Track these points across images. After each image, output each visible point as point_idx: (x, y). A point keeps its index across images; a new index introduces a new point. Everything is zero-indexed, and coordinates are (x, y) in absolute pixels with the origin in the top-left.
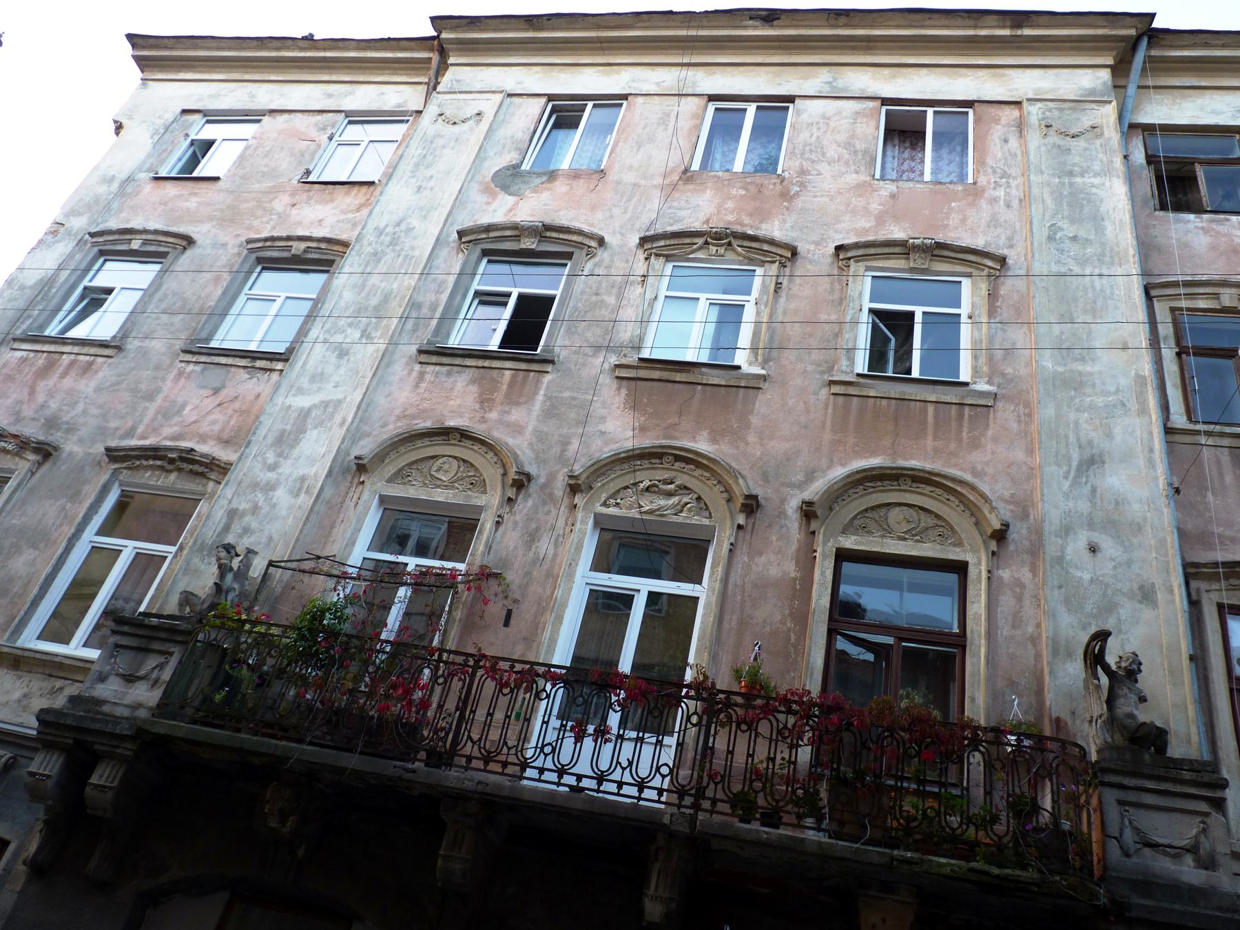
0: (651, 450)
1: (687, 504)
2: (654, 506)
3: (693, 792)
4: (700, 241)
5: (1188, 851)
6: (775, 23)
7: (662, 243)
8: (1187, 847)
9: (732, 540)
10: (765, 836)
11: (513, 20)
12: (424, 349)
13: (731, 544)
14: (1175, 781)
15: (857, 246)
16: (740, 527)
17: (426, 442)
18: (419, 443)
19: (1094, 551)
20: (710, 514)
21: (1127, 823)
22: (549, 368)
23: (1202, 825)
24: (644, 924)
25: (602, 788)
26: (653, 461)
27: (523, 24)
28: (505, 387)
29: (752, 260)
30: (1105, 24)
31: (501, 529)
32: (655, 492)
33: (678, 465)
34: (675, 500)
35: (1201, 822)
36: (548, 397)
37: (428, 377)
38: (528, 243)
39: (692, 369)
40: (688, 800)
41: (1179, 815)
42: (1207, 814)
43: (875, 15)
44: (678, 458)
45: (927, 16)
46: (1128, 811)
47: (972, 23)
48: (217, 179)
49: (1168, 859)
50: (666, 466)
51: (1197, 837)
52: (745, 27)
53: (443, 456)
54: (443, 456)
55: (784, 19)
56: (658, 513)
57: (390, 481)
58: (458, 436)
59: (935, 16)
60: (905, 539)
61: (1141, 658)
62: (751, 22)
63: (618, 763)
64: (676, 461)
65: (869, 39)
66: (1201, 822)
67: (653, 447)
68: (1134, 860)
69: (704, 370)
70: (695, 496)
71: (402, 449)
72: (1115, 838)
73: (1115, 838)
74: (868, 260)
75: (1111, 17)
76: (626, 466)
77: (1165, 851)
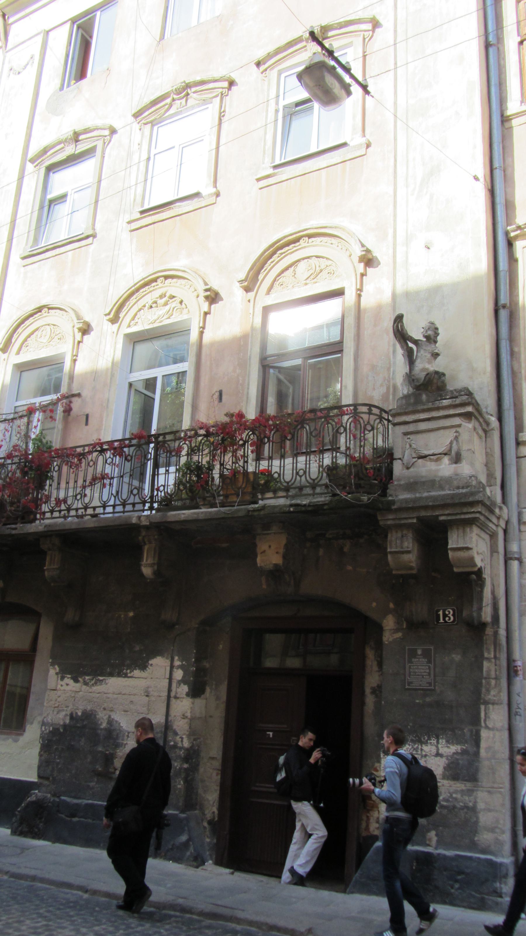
1: (174, 308)
2: (155, 317)
3: (149, 500)
4: (168, 101)
5: (445, 454)
8: (444, 452)
10: (183, 516)
12: (22, 256)
14: (438, 409)
15: (269, 56)
17: (31, 320)
19: (428, 248)
20: (189, 311)
21: (408, 446)
23: (455, 434)
24: (148, 581)
25: (106, 511)
29: (204, 100)
34: (167, 308)
35: (455, 432)
38: (70, 150)
39: (172, 206)
40: (147, 505)
41: (442, 431)
42: (459, 426)
44: (166, 277)
46: (409, 438)
49: (433, 463)
51: (451, 443)
53: (42, 326)
54: (42, 326)
56: (158, 321)
58: (46, 309)
60: (306, 284)
61: (438, 326)
63: (112, 494)
66: (455, 432)
68: (411, 470)
69: (178, 204)
70: (180, 300)
72: (400, 459)
73: (400, 459)
74: (277, 66)
77: (430, 459)
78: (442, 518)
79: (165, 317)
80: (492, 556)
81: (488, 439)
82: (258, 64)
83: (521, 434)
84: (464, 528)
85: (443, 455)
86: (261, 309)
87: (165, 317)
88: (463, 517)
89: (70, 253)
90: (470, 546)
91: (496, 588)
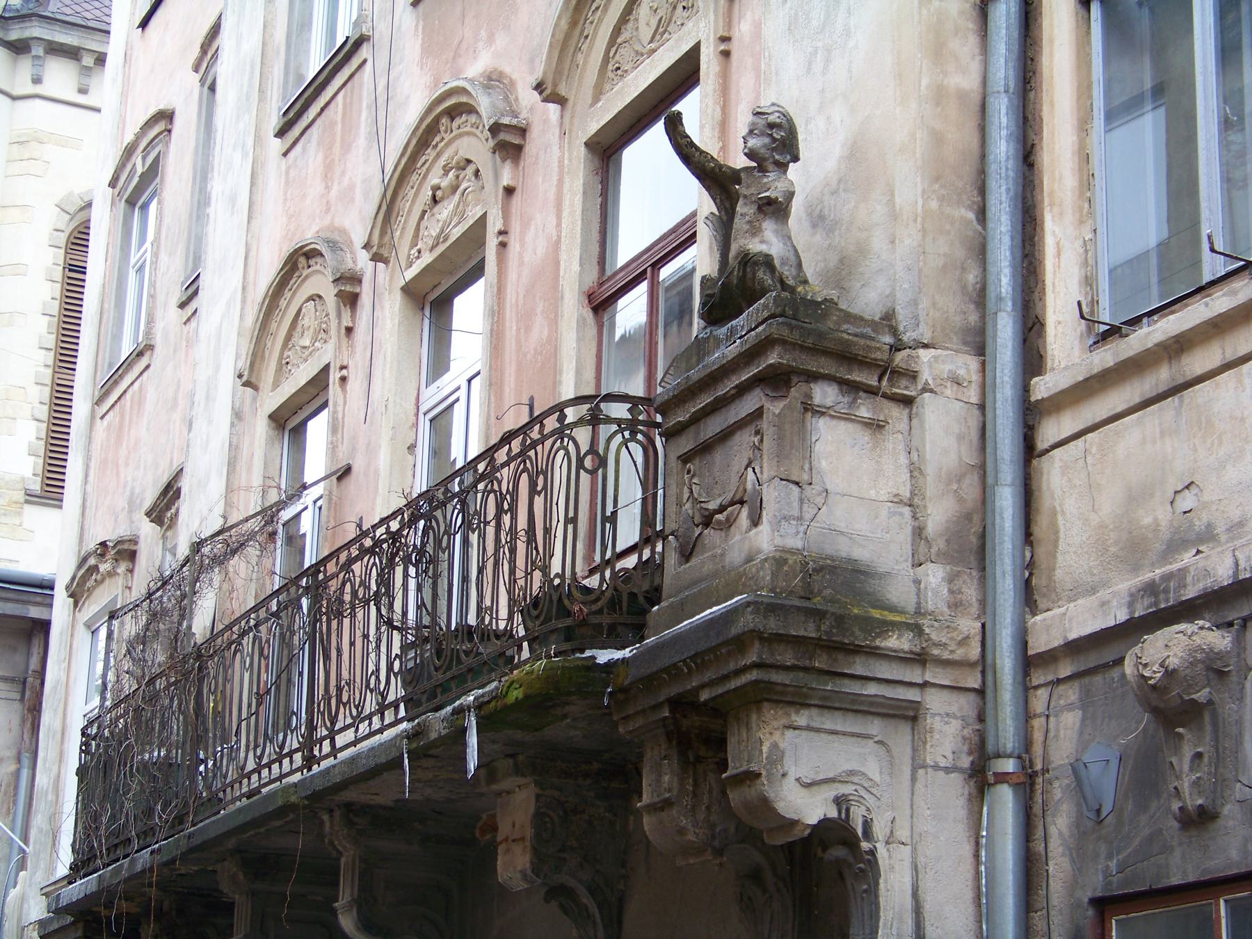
0: (423, 126)
8: (737, 497)
9: (499, 225)
13: (501, 233)
16: (509, 191)
17: (288, 294)
18: (283, 303)
22: (365, 52)
26: (434, 143)
31: (349, 386)
32: (443, 199)
33: (457, 122)
37: (292, 173)
42: (758, 414)
50: (448, 137)
57: (276, 384)
60: (654, 51)
64: (452, 119)
67: (422, 120)
71: (274, 325)
76: (414, 177)
78: (704, 696)
79: (453, 224)
80: (914, 779)
81: (915, 421)
83: (1036, 380)
84: (747, 715)
85: (738, 506)
86: (583, 149)
87: (453, 224)
88: (734, 684)
90: (754, 767)
91: (920, 876)
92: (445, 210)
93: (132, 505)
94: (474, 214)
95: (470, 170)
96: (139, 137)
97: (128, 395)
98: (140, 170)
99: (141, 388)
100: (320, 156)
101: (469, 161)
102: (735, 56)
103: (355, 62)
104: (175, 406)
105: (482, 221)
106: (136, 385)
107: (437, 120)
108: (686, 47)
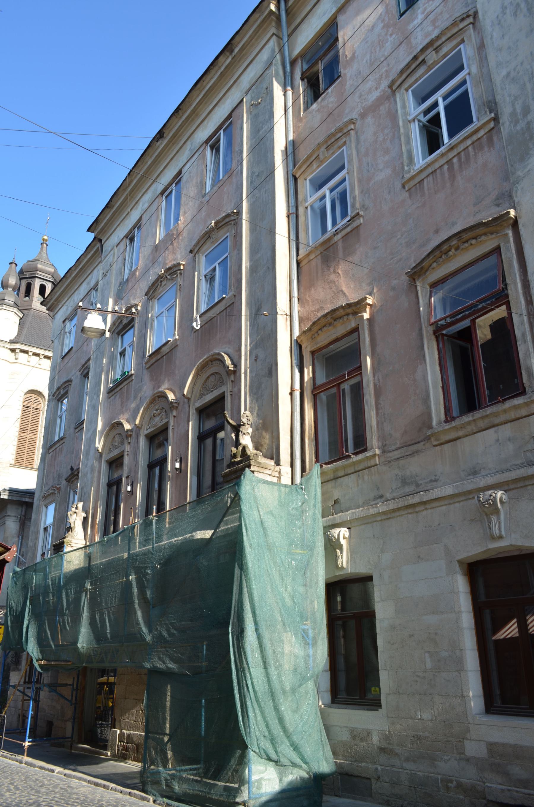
6: (165, 136)
7: (151, 292)
11: (104, 211)
15: (195, 246)
27: (108, 210)
28: (125, 394)
30: (258, 15)
36: (134, 391)
37: (111, 403)
43: (187, 99)
45: (202, 81)
47: (217, 68)
48: (72, 348)
52: (159, 147)
55: (166, 131)
59: (204, 78)
60: (212, 391)
62: (158, 143)
65: (193, 111)
75: (257, 10)
82: (191, 251)
89: (126, 387)
92: (157, 419)
93: (59, 476)
94: (165, 421)
95: (164, 411)
96: (62, 385)
97: (58, 449)
98: (62, 393)
99: (62, 447)
100: (120, 400)
101: (163, 408)
102: (233, 395)
103: (130, 379)
104: (73, 453)
105: (167, 423)
106: (61, 446)
107: (155, 398)
108: (221, 392)
